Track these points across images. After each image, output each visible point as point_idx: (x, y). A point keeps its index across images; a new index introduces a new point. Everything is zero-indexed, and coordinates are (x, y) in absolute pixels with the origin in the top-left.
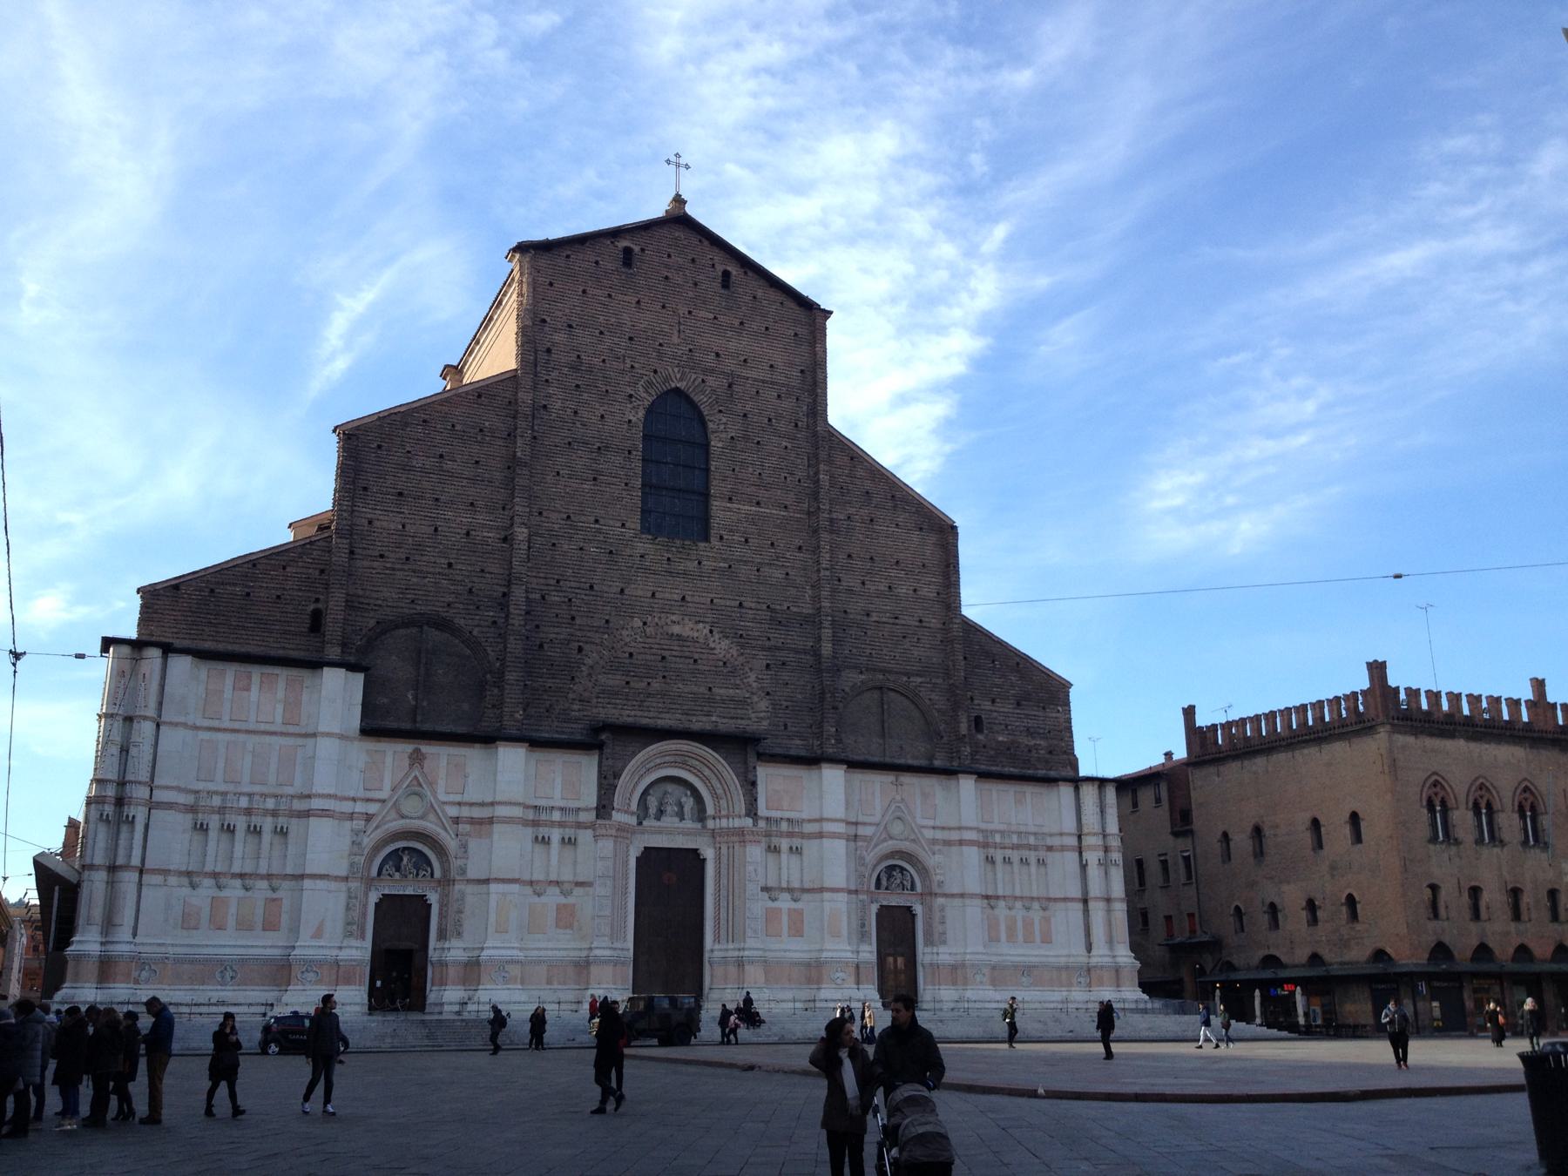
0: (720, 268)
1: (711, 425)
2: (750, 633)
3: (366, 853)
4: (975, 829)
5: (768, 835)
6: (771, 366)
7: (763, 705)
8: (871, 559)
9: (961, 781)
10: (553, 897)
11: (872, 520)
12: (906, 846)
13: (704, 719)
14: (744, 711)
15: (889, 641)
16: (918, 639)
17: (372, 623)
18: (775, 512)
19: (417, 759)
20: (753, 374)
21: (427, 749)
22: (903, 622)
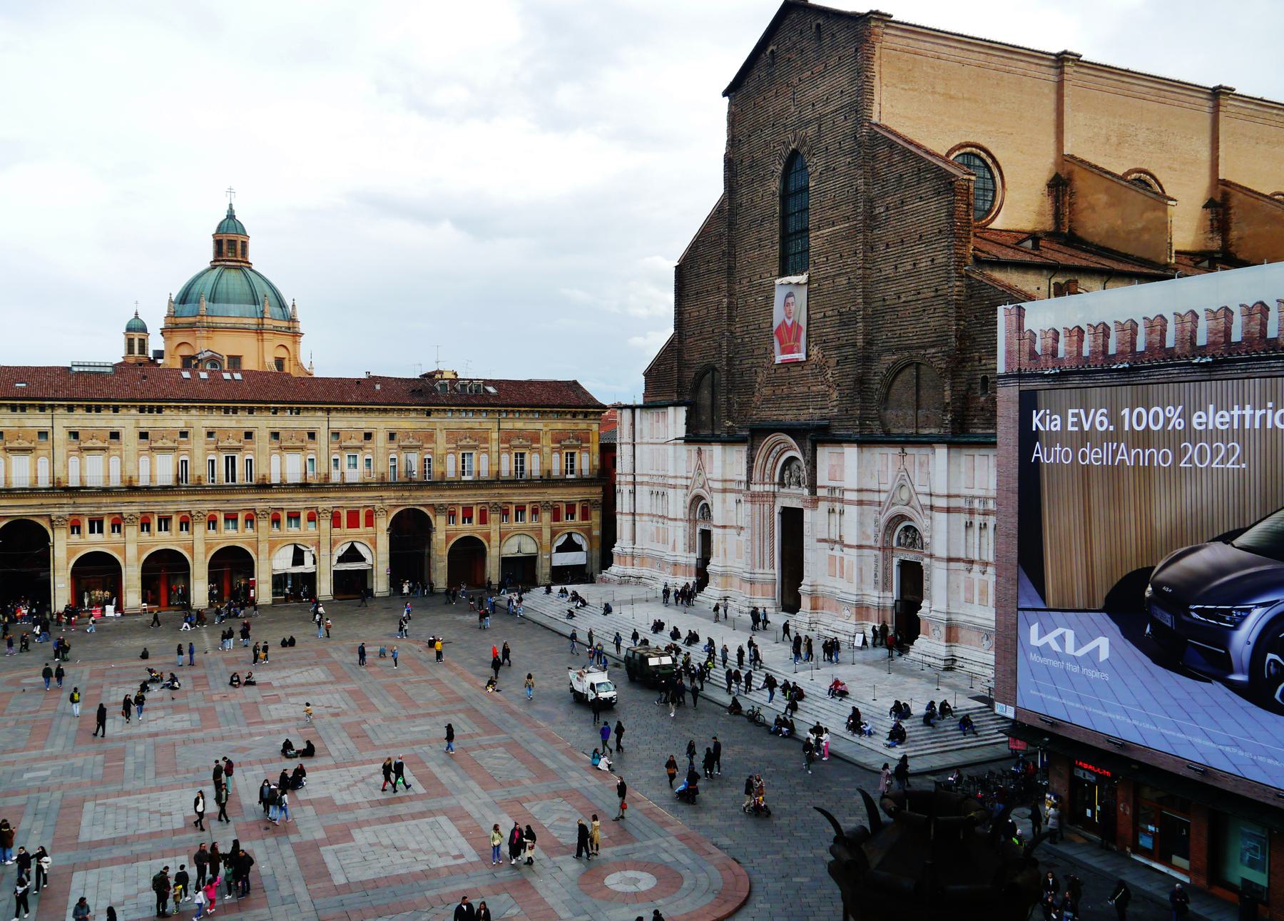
0: (814, 26)
1: (810, 170)
2: (829, 337)
3: (688, 506)
4: (943, 496)
5: (825, 499)
6: (842, 92)
7: (835, 395)
8: (902, 241)
9: (937, 450)
10: (745, 535)
11: (903, 202)
12: (906, 511)
13: (806, 411)
14: (825, 403)
15: (913, 318)
16: (935, 309)
17: (693, 374)
18: (842, 226)
19: (700, 452)
20: (832, 108)
21: (703, 447)
22: (923, 296)
